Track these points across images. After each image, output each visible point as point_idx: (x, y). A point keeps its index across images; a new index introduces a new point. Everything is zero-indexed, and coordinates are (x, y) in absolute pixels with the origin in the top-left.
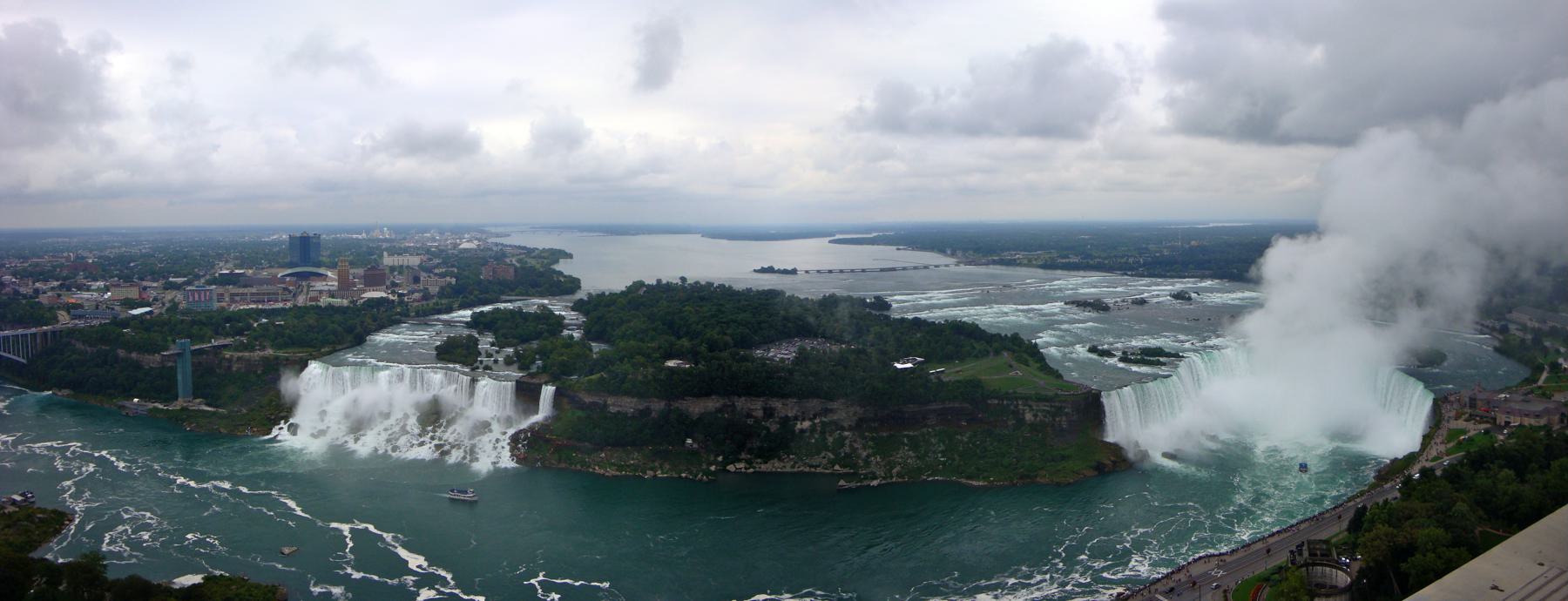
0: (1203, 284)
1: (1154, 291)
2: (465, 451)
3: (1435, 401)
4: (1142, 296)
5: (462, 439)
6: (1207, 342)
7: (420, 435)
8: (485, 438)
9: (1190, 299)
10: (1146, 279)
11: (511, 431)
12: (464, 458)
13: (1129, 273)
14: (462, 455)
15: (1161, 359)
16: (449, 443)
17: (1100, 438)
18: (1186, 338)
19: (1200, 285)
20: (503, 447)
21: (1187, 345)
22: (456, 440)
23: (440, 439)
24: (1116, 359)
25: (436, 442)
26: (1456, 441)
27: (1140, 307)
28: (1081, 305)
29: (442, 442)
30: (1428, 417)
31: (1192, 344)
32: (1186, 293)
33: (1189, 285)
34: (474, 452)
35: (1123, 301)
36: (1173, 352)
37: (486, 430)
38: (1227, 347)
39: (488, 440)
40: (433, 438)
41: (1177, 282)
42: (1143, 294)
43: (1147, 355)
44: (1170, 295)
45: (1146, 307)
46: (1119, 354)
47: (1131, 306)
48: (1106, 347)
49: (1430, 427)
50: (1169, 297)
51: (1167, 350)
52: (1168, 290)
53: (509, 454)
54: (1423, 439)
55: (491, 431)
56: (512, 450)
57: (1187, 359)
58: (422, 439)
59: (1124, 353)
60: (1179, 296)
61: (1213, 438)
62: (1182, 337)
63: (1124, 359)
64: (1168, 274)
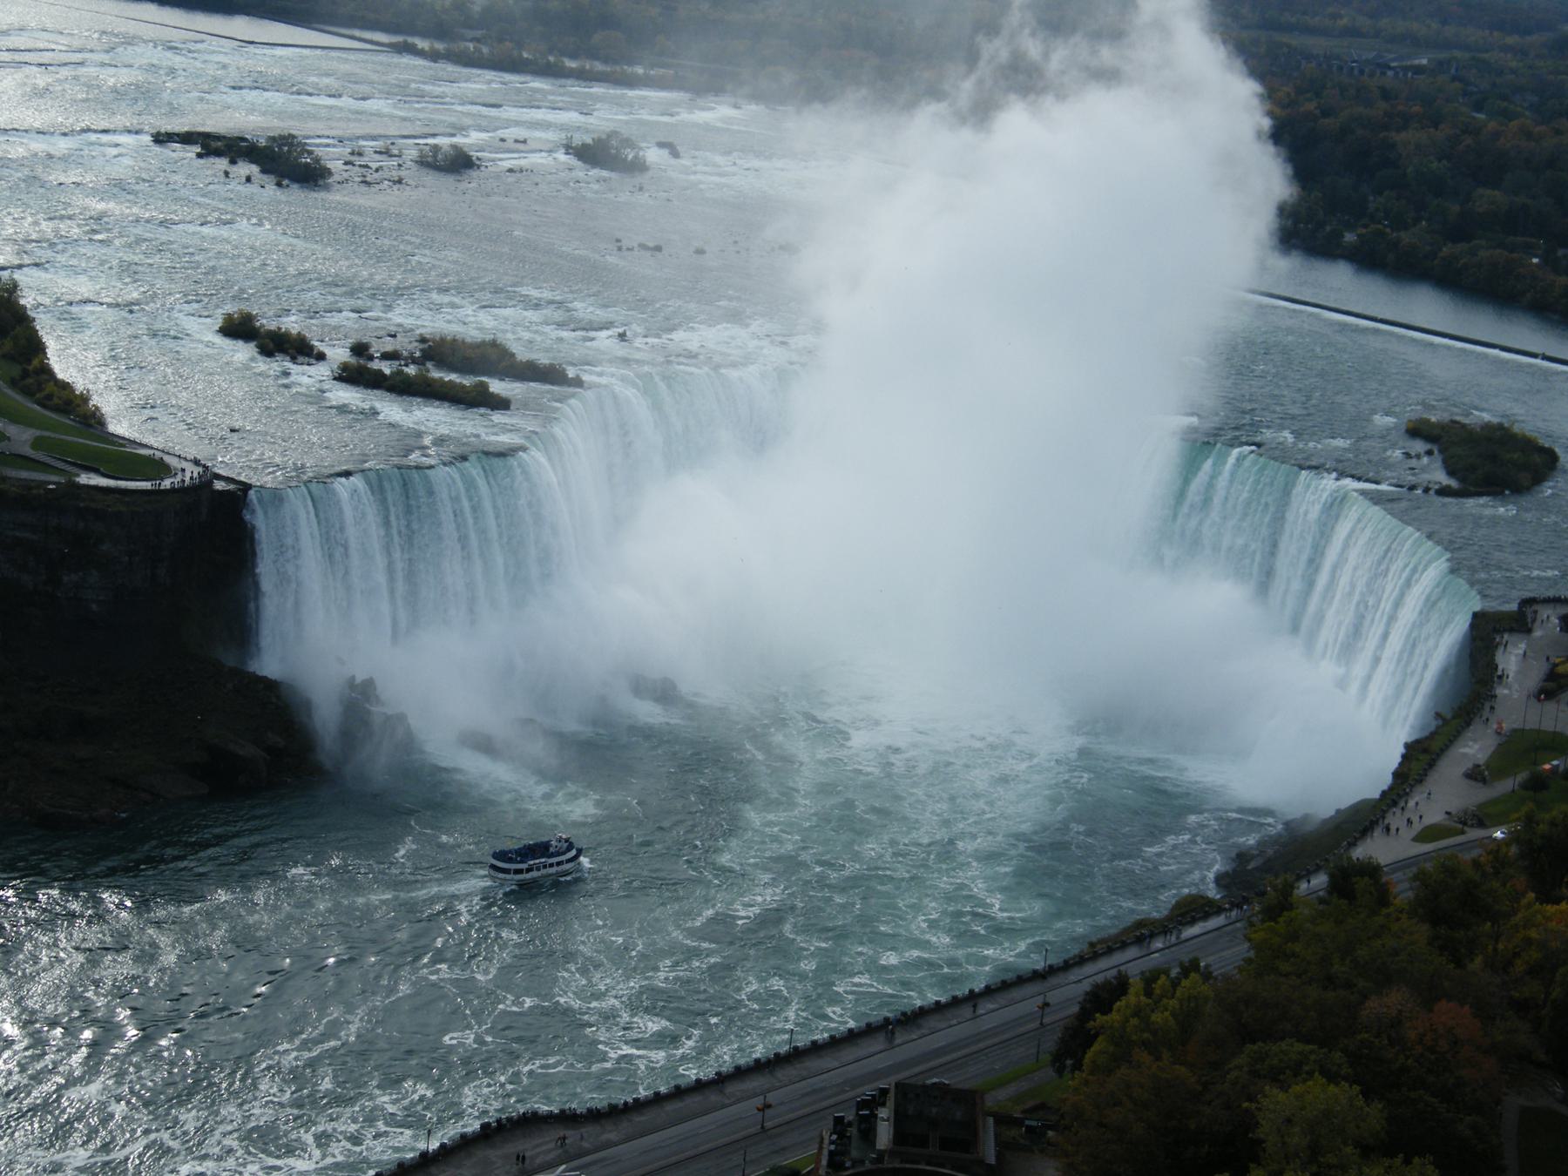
0: (701, 116)
1: (510, 123)
3: (1475, 615)
4: (458, 140)
6: (678, 335)
9: (638, 166)
10: (489, 75)
13: (422, 44)
15: (497, 386)
17: (230, 660)
18: (602, 315)
19: (684, 116)
21: (604, 340)
24: (321, 371)
26: (1522, 776)
27: (448, 181)
28: (218, 153)
30: (1444, 672)
31: (622, 336)
32: (628, 143)
33: (645, 115)
35: (386, 152)
36: (544, 359)
38: (747, 360)
41: (597, 98)
42: (461, 129)
43: (443, 363)
44: (569, 148)
45: (471, 182)
46: (339, 354)
47: (410, 173)
48: (292, 324)
49: (1438, 715)
50: (562, 156)
51: (522, 354)
52: (562, 127)
54: (1404, 757)
57: (589, 394)
59: (360, 350)
60: (593, 153)
61: (665, 693)
62: (584, 309)
63: (352, 376)
64: (571, 64)
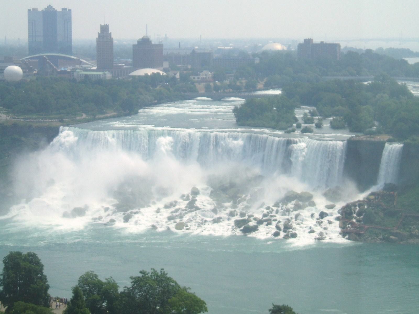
2: (278, 227)
5: (274, 213)
7: (215, 211)
8: (305, 213)
11: (340, 205)
12: (276, 234)
14: (274, 230)
16: (255, 219)
20: (330, 222)
22: (265, 216)
23: (242, 215)
25: (238, 218)
29: (246, 217)
34: (290, 227)
37: (307, 203)
39: (309, 214)
40: (232, 214)
53: (339, 230)
55: (313, 204)
56: (343, 227)
58: (216, 216)
